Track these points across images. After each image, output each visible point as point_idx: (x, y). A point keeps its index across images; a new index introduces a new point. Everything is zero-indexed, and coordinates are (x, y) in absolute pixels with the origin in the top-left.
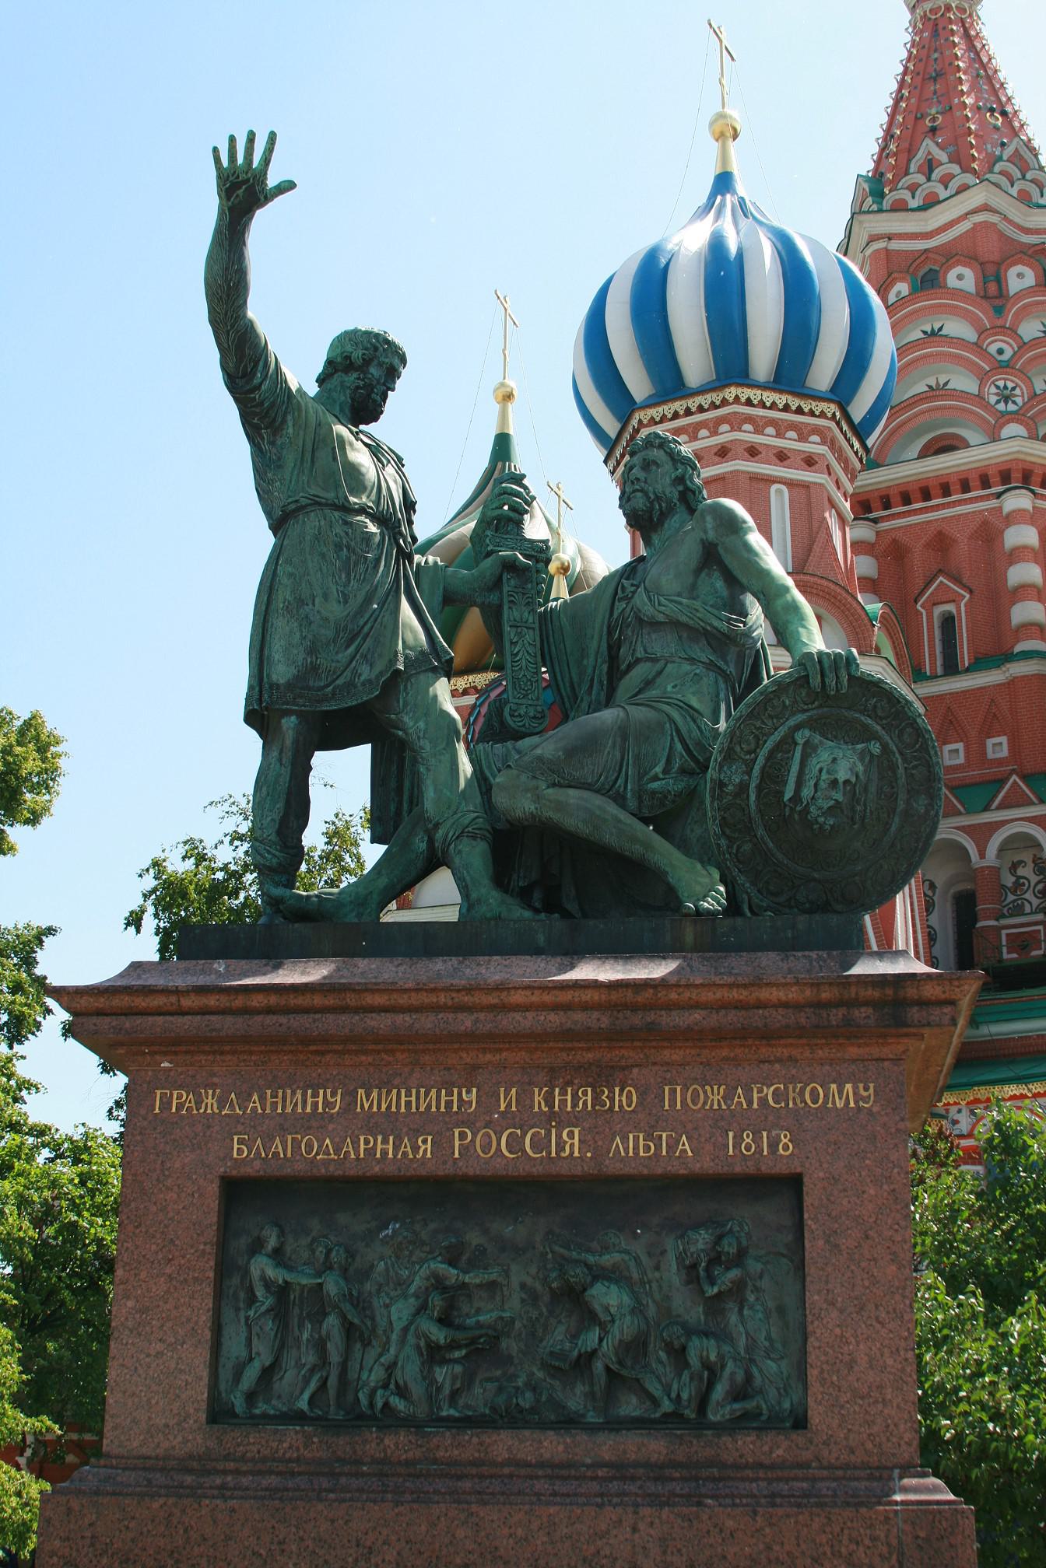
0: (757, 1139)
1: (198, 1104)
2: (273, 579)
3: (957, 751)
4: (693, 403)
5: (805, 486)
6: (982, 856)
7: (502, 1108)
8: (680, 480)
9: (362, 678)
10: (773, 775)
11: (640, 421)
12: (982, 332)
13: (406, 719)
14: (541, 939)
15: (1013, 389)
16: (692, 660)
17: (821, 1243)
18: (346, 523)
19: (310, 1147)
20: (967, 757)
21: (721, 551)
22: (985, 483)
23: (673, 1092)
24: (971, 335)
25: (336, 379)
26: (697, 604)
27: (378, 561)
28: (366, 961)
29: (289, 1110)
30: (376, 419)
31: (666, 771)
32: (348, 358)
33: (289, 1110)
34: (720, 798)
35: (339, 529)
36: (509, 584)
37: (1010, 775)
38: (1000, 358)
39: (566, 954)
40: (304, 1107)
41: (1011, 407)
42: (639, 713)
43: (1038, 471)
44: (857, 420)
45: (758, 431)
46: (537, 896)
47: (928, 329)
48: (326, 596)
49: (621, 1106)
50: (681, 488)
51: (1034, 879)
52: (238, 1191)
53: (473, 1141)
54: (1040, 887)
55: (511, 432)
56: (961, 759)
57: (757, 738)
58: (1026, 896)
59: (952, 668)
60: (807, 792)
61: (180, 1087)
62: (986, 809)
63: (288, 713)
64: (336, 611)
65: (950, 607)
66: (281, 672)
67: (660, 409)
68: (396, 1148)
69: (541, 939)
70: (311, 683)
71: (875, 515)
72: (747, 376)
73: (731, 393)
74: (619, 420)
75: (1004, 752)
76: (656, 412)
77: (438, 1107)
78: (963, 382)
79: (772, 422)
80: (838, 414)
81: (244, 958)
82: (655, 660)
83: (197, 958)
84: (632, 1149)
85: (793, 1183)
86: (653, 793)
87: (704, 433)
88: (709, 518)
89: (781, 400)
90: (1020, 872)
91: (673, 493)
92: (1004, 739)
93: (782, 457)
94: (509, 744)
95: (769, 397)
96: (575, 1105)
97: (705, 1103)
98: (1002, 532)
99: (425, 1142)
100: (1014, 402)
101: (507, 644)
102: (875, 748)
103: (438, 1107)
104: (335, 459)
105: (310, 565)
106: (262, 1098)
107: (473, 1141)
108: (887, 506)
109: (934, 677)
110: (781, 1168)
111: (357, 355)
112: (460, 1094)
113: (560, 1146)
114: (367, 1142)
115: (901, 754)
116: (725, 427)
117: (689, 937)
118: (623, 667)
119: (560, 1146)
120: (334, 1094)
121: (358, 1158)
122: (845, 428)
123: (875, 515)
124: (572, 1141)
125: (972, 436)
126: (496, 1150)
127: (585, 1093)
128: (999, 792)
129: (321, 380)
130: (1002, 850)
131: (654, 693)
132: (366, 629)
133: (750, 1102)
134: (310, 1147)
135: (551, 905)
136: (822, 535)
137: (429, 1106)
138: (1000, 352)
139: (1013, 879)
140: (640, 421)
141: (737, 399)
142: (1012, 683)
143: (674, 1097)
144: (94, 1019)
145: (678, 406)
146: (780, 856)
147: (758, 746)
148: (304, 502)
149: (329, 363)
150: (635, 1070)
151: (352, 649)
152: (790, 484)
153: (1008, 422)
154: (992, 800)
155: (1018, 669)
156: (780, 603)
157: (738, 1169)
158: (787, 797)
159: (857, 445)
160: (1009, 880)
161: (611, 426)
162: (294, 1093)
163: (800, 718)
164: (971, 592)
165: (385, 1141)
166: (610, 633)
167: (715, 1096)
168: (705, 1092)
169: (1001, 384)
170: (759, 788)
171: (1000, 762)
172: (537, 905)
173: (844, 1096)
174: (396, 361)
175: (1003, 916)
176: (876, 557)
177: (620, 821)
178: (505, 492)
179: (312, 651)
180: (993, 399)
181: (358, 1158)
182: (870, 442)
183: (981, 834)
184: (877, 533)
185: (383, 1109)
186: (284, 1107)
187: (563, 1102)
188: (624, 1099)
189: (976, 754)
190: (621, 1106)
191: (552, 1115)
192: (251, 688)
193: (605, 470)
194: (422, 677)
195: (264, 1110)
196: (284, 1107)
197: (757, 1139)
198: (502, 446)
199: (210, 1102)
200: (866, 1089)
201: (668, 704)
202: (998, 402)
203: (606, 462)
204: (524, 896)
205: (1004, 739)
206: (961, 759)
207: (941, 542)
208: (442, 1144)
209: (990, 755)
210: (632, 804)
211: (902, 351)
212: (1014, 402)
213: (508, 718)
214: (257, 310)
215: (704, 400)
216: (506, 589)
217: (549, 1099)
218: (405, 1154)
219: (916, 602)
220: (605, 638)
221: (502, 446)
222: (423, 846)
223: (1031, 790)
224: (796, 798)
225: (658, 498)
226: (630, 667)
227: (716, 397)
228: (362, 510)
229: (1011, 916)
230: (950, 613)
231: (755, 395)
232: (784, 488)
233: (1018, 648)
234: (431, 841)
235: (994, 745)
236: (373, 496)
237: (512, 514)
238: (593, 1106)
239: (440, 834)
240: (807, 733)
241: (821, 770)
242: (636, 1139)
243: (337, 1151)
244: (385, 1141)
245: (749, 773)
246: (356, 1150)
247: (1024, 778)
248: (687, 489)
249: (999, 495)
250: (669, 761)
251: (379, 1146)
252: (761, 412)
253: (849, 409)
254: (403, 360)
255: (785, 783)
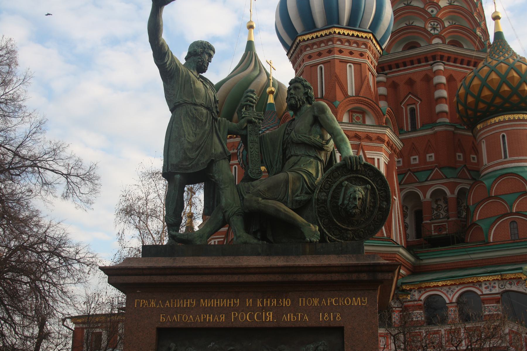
0: (329, 315)
1: (149, 304)
2: (171, 129)
3: (416, 159)
4: (319, 34)
5: (360, 64)
6: (425, 196)
7: (247, 305)
8: (306, 93)
9: (201, 162)
10: (335, 197)
11: (300, 40)
12: (426, 4)
13: (215, 175)
14: (260, 250)
15: (437, 25)
16: (310, 156)
17: (350, 349)
18: (195, 109)
19: (185, 318)
20: (419, 161)
21: (319, 119)
22: (426, 60)
23: (302, 300)
24: (421, 5)
25: (192, 58)
26: (312, 137)
27: (206, 122)
28: (203, 258)
29: (178, 306)
30: (205, 72)
31: (301, 193)
32: (195, 51)
33: (178, 306)
34: (318, 205)
35: (194, 111)
36: (250, 127)
37: (435, 168)
38: (432, 14)
39: (268, 255)
40: (183, 305)
41: (436, 32)
42: (291, 175)
43: (446, 55)
44: (378, 39)
45: (342, 43)
46: (259, 235)
47: (406, 3)
48: (189, 134)
49: (285, 305)
50: (306, 96)
51: (444, 205)
52: (164, 333)
53: (238, 316)
54: (446, 208)
55: (253, 40)
56: (417, 162)
57: (330, 184)
58: (441, 212)
59: (414, 128)
60: (346, 202)
61: (143, 299)
62: (426, 180)
63: (177, 173)
64: (192, 139)
65: (413, 106)
66: (174, 161)
67: (307, 36)
68: (213, 319)
69: (260, 250)
70: (184, 164)
71: (386, 72)
72: (338, 23)
73: (332, 31)
74: (292, 40)
75: (433, 159)
76: (306, 37)
77: (227, 305)
78: (419, 24)
79: (348, 41)
80: (372, 37)
81: (163, 256)
82: (298, 156)
83: (148, 256)
84: (289, 318)
85: (341, 329)
86: (297, 201)
87: (323, 45)
88: (315, 108)
89: (351, 33)
90: (439, 203)
91: (304, 98)
92: (433, 154)
93: (351, 53)
94: (249, 183)
95: (346, 32)
96: (271, 304)
97: (312, 304)
98: (432, 79)
99: (222, 316)
100: (437, 30)
101: (249, 149)
102: (369, 186)
103: (227, 305)
104: (191, 88)
105: (183, 124)
106: (170, 302)
107: (238, 316)
108: (390, 69)
109: (408, 132)
110: (337, 325)
111: (199, 50)
112: (234, 301)
113: (266, 318)
114: (204, 316)
115: (377, 188)
116: (330, 43)
117: (308, 250)
118: (287, 157)
119: (266, 318)
120: (193, 301)
121: (201, 322)
122: (374, 42)
123: (386, 72)
124: (270, 316)
125: (422, 44)
126: (246, 318)
127: (274, 301)
128: (431, 174)
129: (186, 59)
130: (431, 196)
131: (297, 167)
132: (202, 145)
133: (327, 304)
134: (185, 318)
135: (264, 238)
136: (366, 83)
137: (224, 305)
138: (432, 11)
139: (436, 205)
140: (300, 40)
141: (335, 32)
142: (436, 133)
143: (302, 302)
144: (115, 277)
145: (314, 35)
146: (337, 223)
147: (330, 186)
148: (181, 102)
149: (189, 53)
150: (290, 293)
151: (197, 152)
152: (354, 63)
153: (435, 37)
154: (428, 177)
155: (437, 129)
156: (338, 138)
157: (323, 325)
158: (340, 202)
159: (379, 48)
160: (435, 206)
161: (289, 43)
162: (180, 301)
163: (343, 178)
164: (421, 100)
165: (210, 316)
166: (283, 145)
167: (316, 301)
168: (313, 300)
169: (432, 23)
170: (331, 201)
171: (432, 163)
172: (259, 237)
173: (356, 301)
174: (212, 52)
175: (432, 219)
176: (386, 88)
177: (285, 210)
178: (248, 96)
179: (185, 153)
180: (429, 29)
181: (201, 322)
182: (383, 47)
183: (424, 190)
184: (387, 78)
185: (209, 305)
186: (177, 305)
187: (267, 304)
188: (286, 303)
189: (423, 160)
190: (285, 305)
191: (263, 308)
192: (164, 165)
193: (287, 57)
194: (221, 161)
195: (170, 306)
196: (177, 305)
197: (329, 315)
198: (250, 45)
199: (153, 303)
200: (364, 299)
201: (302, 171)
202: (431, 30)
203: (287, 55)
204: (255, 234)
205: (433, 154)
206: (417, 162)
207: (411, 82)
208: (228, 317)
209: (428, 160)
210: (290, 205)
211: (395, 12)
212: (437, 30)
213: (249, 174)
214: (164, 36)
215: (323, 33)
216: (248, 129)
217: (262, 303)
218: (216, 320)
219: (401, 104)
220: (281, 147)
221: (250, 45)
222: (221, 217)
223: (443, 173)
224: (343, 204)
225: (299, 100)
226: (289, 157)
227: (327, 32)
228: (201, 105)
229: (436, 219)
230: (413, 108)
231: (342, 31)
232: (352, 65)
233: (438, 121)
234: (224, 216)
235: (430, 157)
236: (205, 100)
237: (250, 103)
238: (277, 305)
239: (227, 214)
240: (346, 182)
241: (351, 194)
242: (290, 315)
243: (194, 319)
244: (210, 316)
245: (327, 196)
246: (200, 319)
247: (440, 169)
248: (308, 97)
249: (431, 65)
250: (302, 190)
251: (208, 318)
252: (343, 37)
253: (376, 35)
254: (214, 52)
255: (339, 199)
